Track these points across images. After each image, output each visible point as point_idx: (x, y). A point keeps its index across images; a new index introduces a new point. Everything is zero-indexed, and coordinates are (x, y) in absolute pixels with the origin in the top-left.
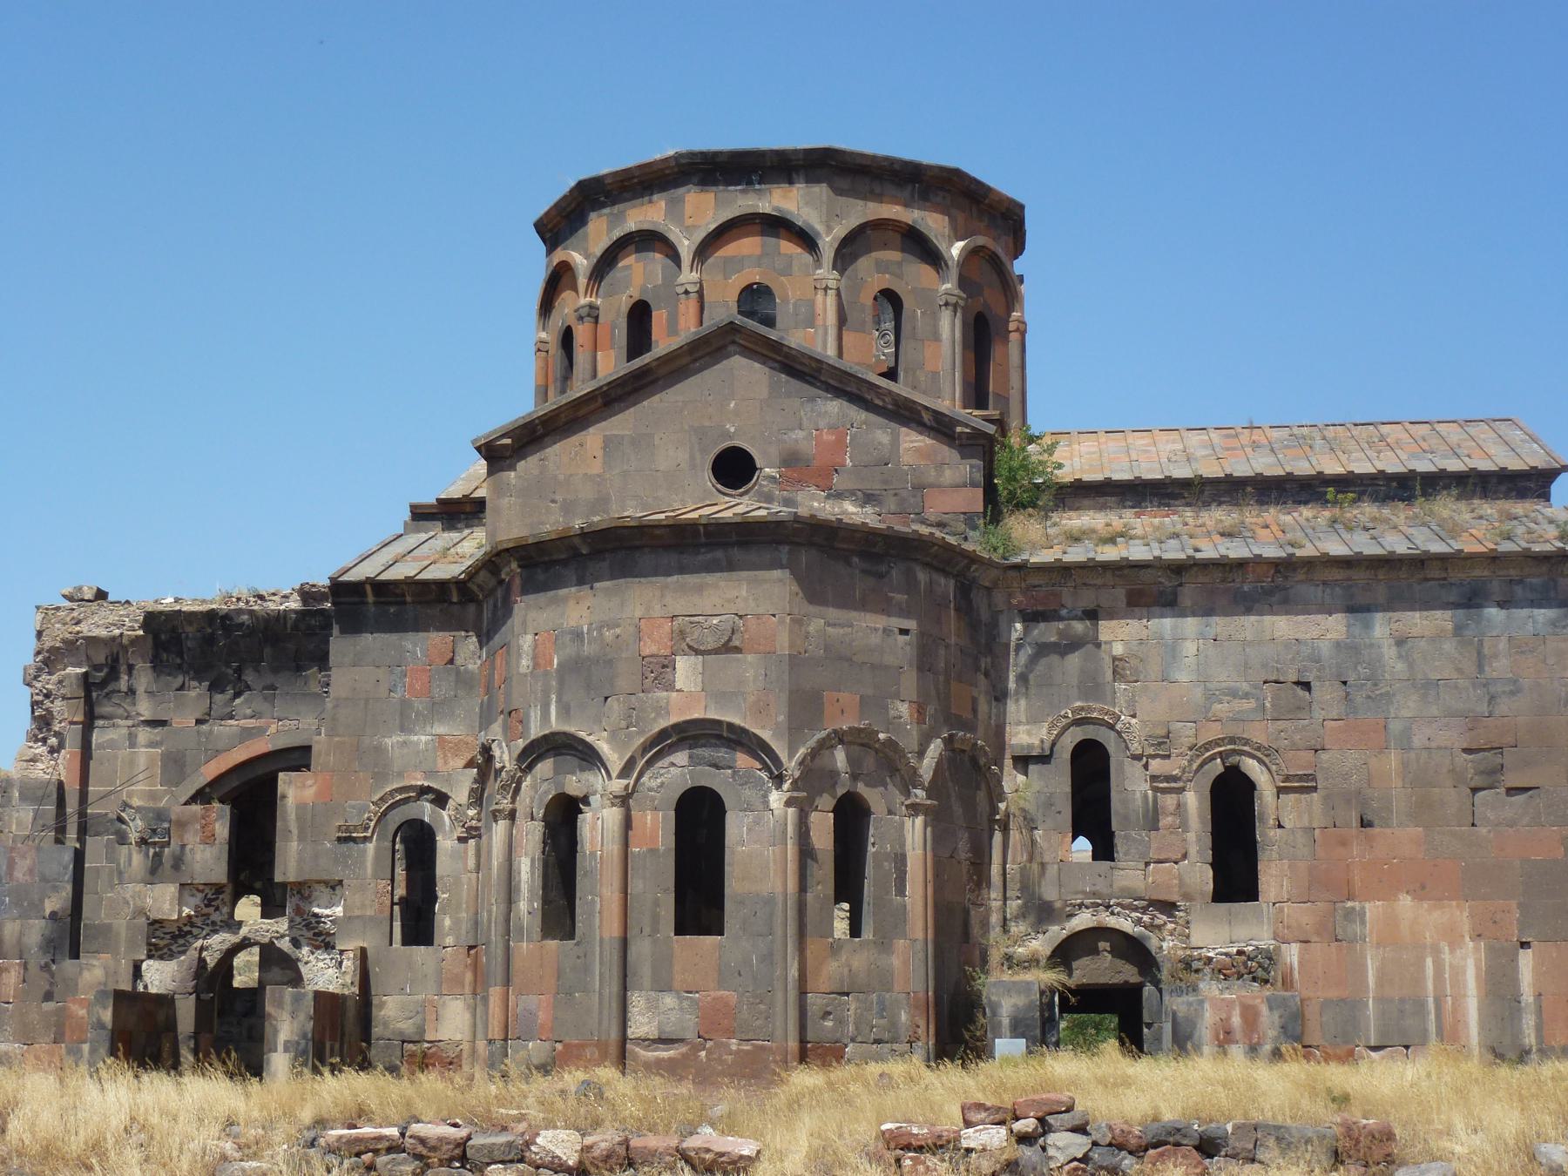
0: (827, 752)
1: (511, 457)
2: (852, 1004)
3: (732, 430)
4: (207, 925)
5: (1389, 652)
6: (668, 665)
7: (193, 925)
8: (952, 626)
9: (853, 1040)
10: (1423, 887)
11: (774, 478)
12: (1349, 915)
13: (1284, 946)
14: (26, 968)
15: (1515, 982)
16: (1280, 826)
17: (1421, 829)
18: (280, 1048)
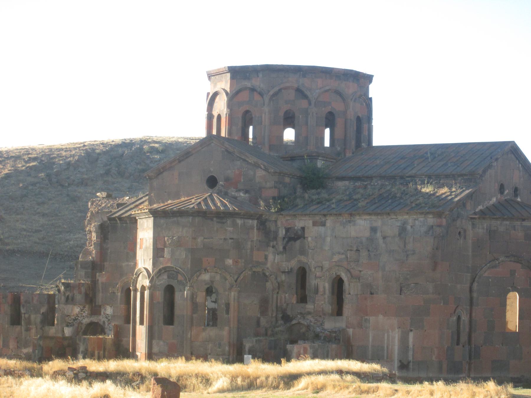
0: (203, 275)
1: (155, 178)
2: (210, 345)
3: (212, 170)
4: (82, 317)
5: (381, 241)
6: (163, 250)
7: (78, 317)
8: (255, 235)
9: (210, 354)
10: (386, 313)
11: (222, 185)
12: (366, 320)
13: (348, 329)
14: (37, 329)
15: (408, 341)
16: (350, 294)
17: (386, 295)
18: (80, 352)
